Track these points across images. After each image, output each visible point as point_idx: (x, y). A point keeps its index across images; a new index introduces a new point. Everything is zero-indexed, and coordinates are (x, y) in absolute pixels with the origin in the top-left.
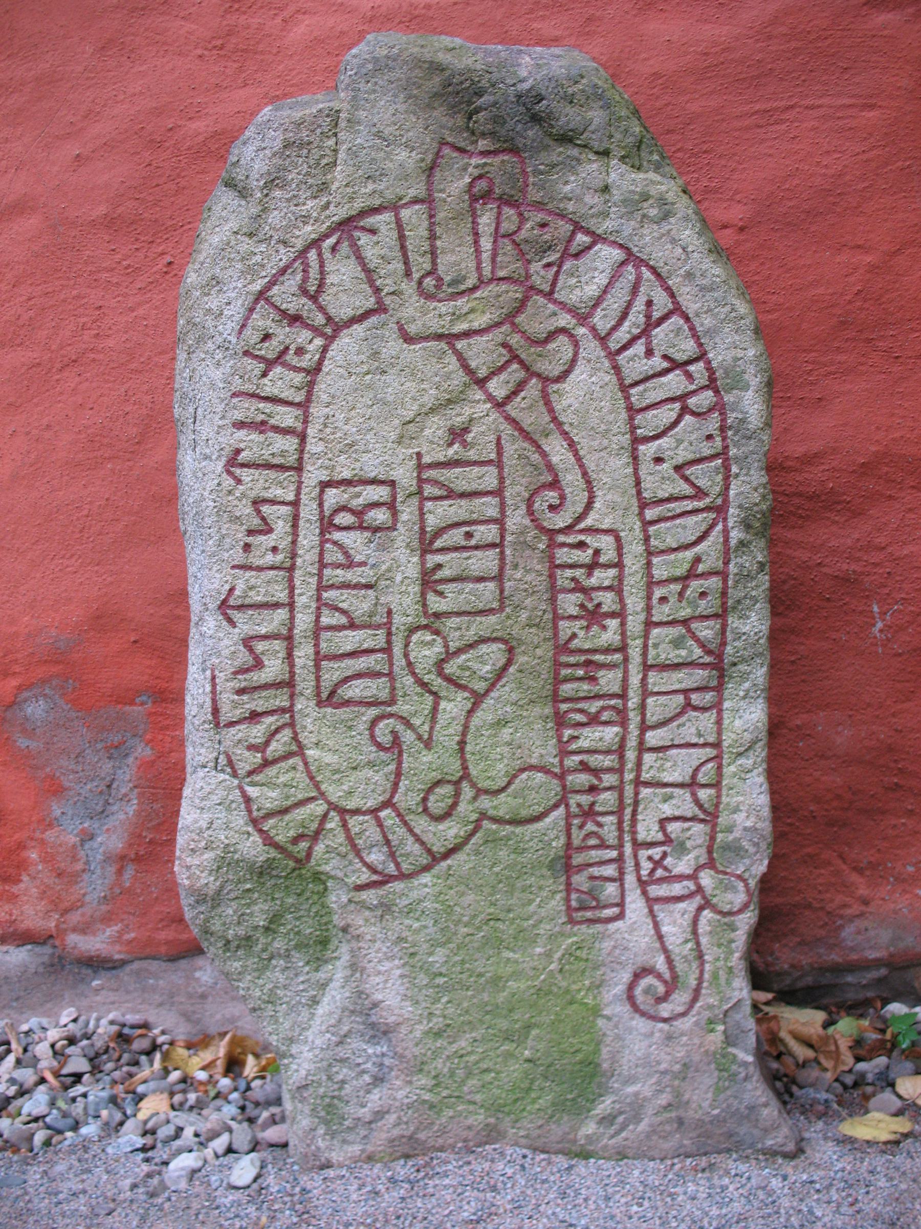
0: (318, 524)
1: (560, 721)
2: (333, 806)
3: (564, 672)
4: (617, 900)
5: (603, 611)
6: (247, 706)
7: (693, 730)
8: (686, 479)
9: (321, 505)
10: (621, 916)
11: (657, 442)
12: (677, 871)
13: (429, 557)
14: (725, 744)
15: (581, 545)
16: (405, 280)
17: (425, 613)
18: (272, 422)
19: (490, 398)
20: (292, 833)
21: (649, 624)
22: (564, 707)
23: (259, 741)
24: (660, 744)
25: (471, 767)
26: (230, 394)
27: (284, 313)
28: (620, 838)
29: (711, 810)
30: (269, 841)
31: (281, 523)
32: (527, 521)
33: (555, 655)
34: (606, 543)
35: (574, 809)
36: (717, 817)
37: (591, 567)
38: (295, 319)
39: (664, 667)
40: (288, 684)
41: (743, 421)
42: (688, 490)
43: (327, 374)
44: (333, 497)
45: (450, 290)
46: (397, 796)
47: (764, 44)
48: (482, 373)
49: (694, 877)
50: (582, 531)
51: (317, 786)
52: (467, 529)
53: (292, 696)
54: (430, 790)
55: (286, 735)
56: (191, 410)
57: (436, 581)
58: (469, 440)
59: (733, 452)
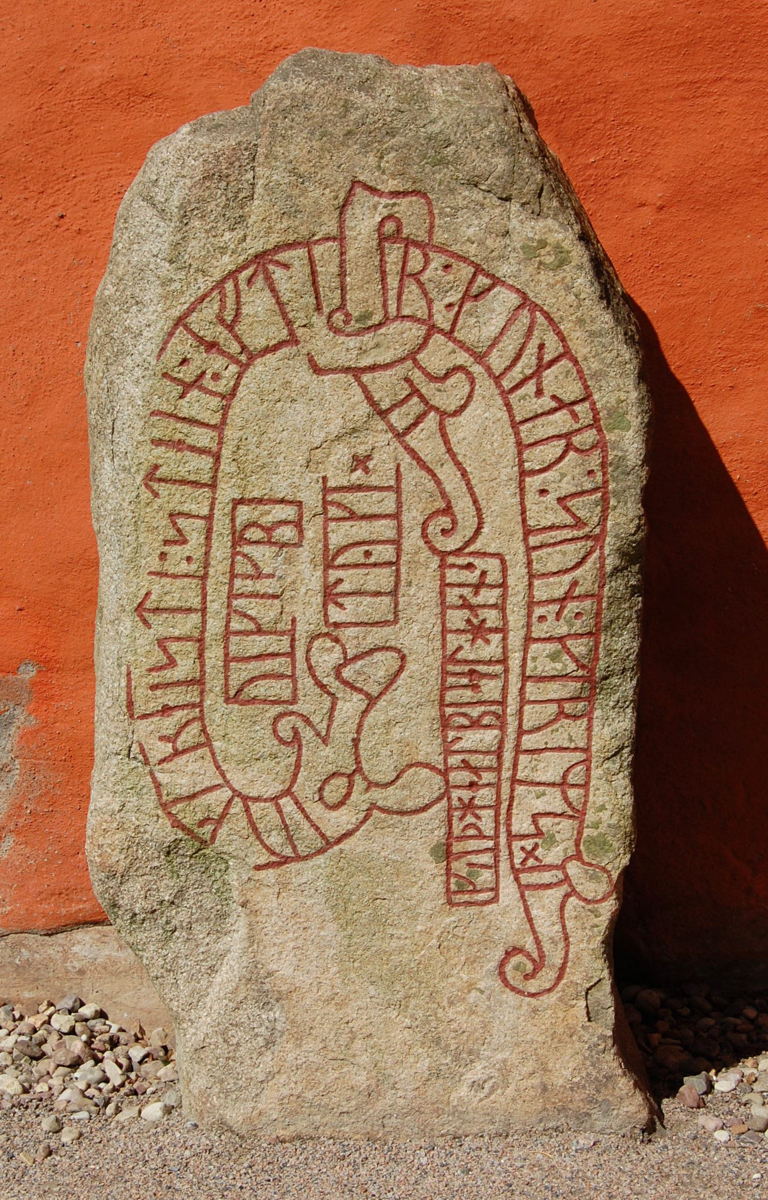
0: (230, 537)
1: (445, 723)
2: (236, 793)
3: (451, 680)
4: (493, 885)
5: (487, 626)
6: (160, 701)
7: (566, 736)
8: (568, 510)
9: (233, 520)
10: (495, 899)
11: (543, 475)
12: (547, 861)
13: (330, 571)
14: (594, 749)
15: (470, 566)
16: (316, 314)
17: (326, 622)
18: (189, 441)
19: (392, 428)
20: (200, 816)
21: (528, 639)
22: (449, 711)
23: (171, 732)
24: (535, 746)
25: (363, 762)
26: (149, 412)
27: (201, 340)
28: (497, 829)
29: (580, 807)
30: (178, 824)
31: (195, 535)
32: (421, 543)
33: (443, 663)
34: (493, 565)
35: (455, 803)
36: (585, 814)
37: (477, 588)
38: (212, 346)
39: (541, 679)
40: (199, 682)
41: (623, 458)
42: (569, 520)
43: (241, 399)
44: (244, 513)
45: (357, 325)
46: (296, 786)
47: (695, 10)
48: (384, 406)
49: (562, 867)
50: (471, 554)
51: (223, 775)
52: (367, 548)
53: (202, 692)
54: (326, 781)
55: (195, 728)
56: (109, 421)
57: (337, 594)
58: (371, 466)
59: (612, 486)
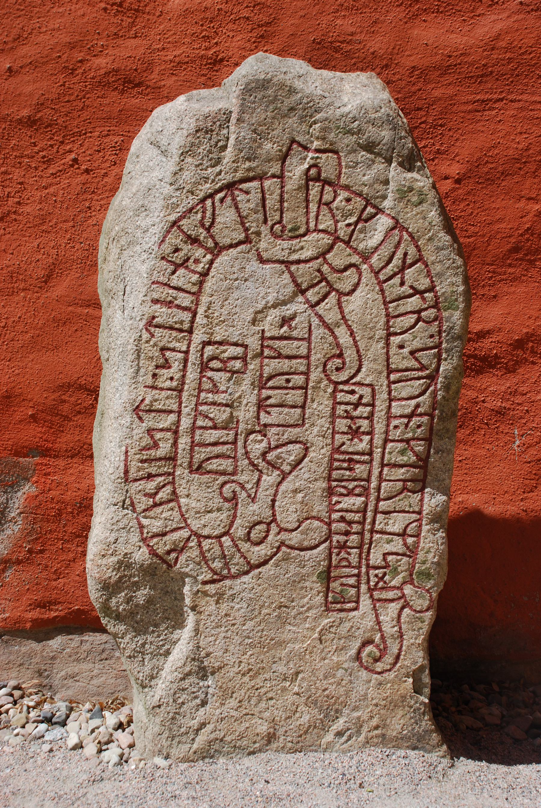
1: (330, 492)
6: (146, 470)
7: (407, 503)
8: (416, 359)
10: (356, 609)
13: (264, 391)
14: (424, 513)
15: (352, 392)
19: (307, 301)
20: (168, 548)
21: (386, 441)
22: (334, 484)
27: (189, 237)
28: (360, 562)
33: (331, 453)
37: (356, 406)
38: (194, 241)
40: (172, 458)
42: (417, 365)
44: (209, 350)
45: (290, 234)
50: (354, 384)
51: (185, 521)
53: (174, 467)
55: (168, 489)
58: (293, 325)
